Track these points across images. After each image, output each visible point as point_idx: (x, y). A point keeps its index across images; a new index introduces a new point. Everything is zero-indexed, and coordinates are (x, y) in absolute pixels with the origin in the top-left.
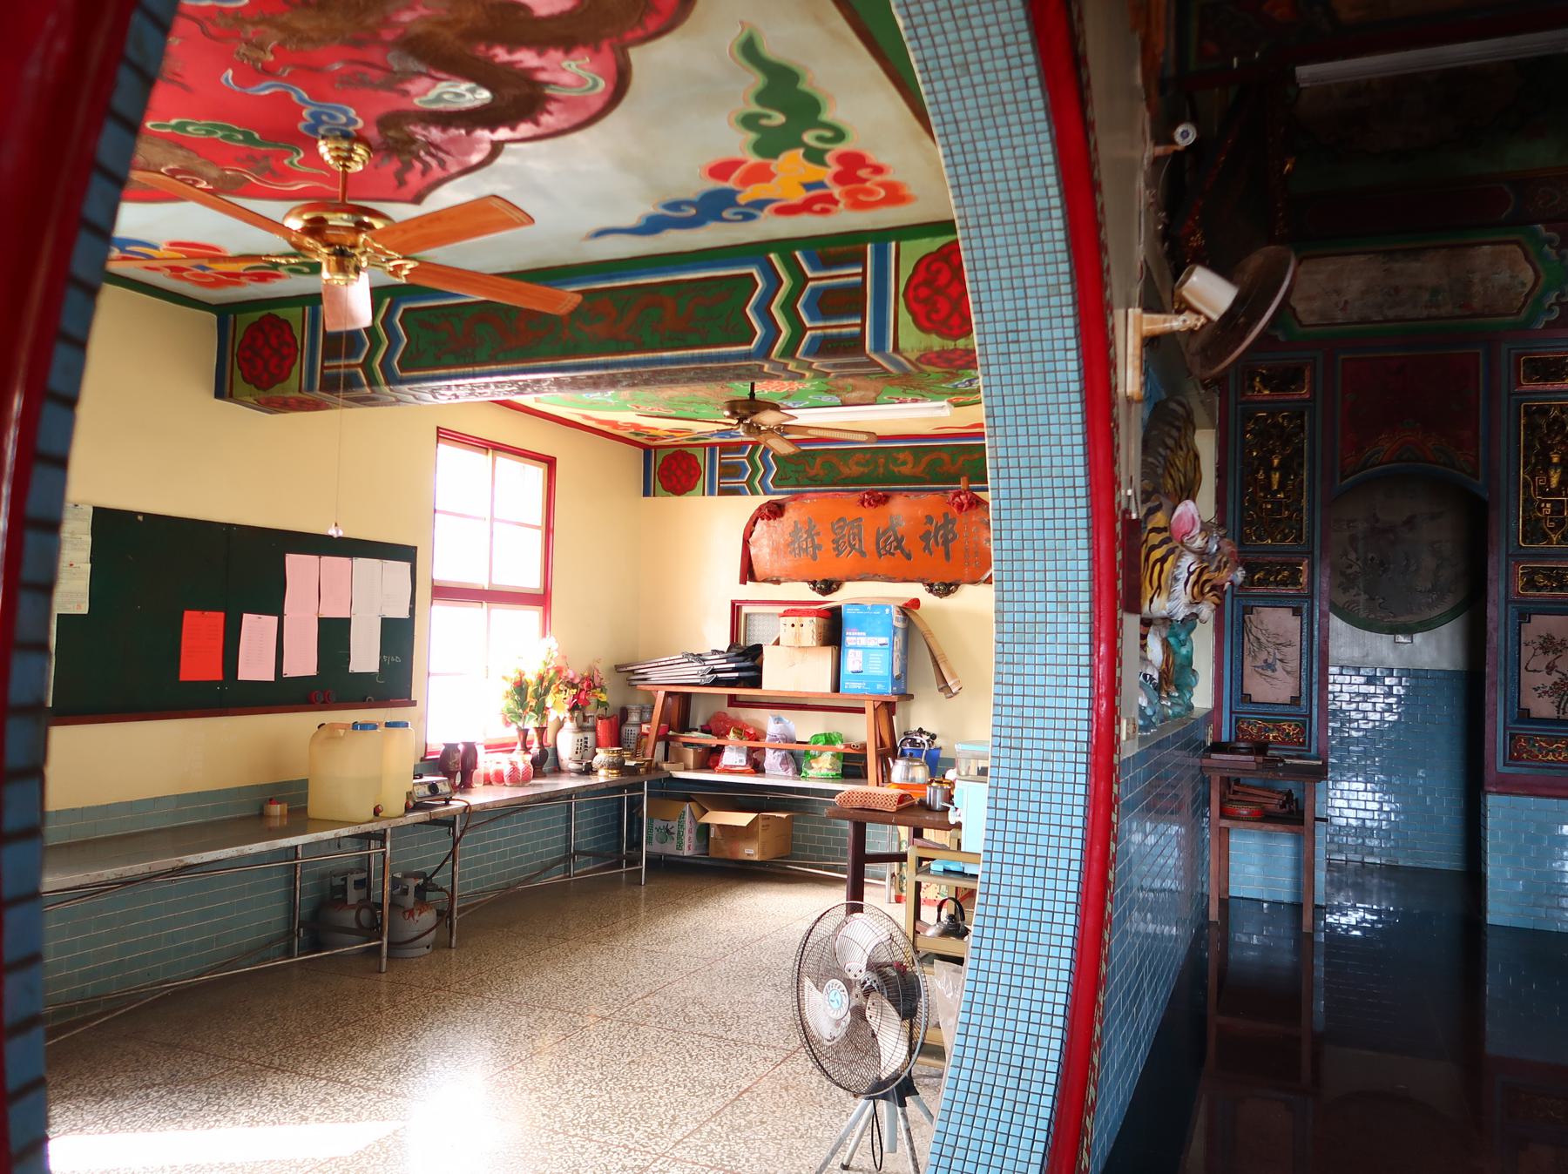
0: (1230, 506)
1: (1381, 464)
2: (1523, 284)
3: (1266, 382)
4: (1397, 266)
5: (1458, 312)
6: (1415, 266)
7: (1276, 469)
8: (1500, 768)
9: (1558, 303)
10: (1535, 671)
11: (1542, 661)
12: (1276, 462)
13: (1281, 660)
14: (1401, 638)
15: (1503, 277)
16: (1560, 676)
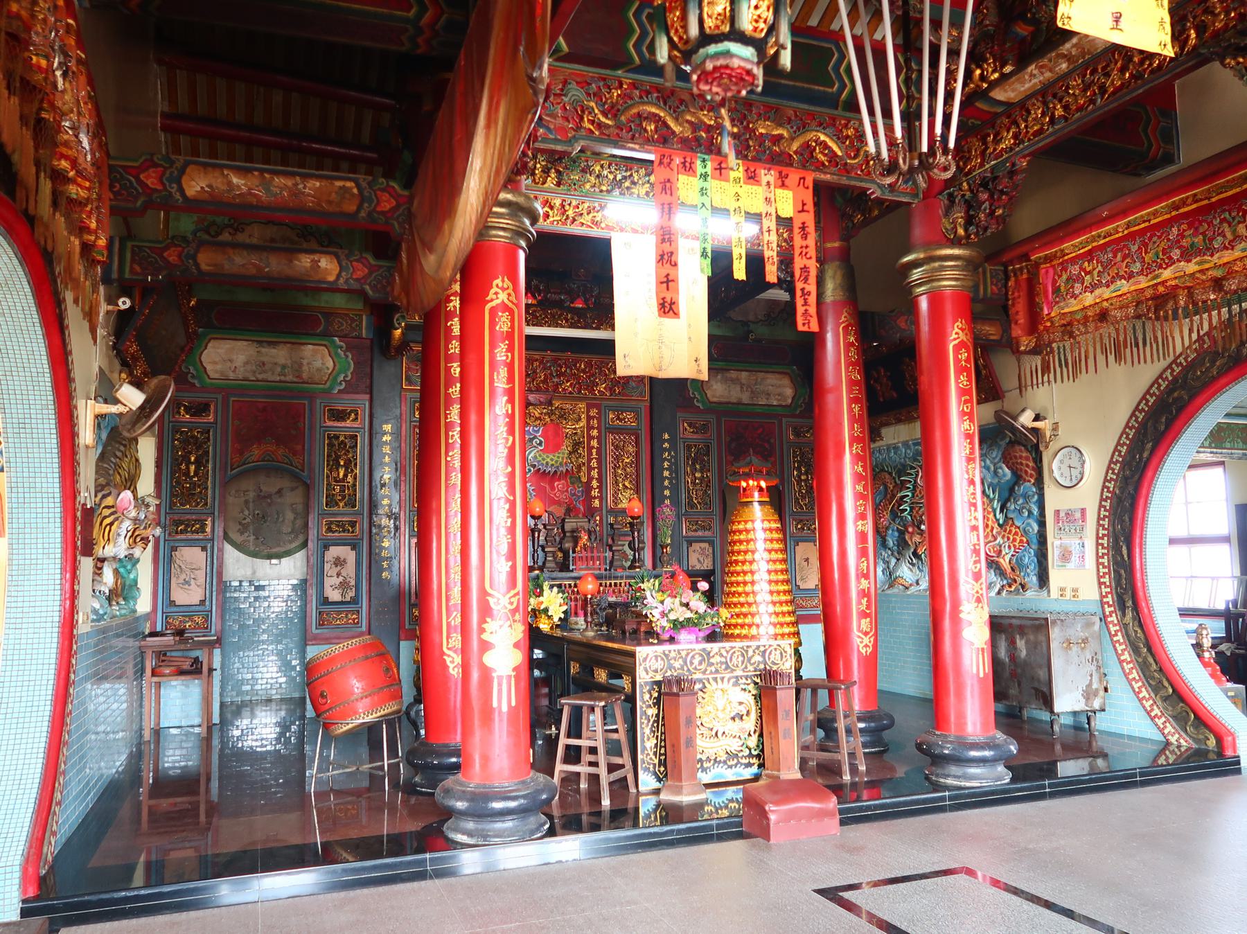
0: (164, 485)
2: (328, 369)
3: (187, 410)
4: (263, 350)
5: (295, 380)
6: (273, 351)
7: (193, 463)
8: (314, 631)
9: (344, 380)
11: (335, 570)
12: (193, 459)
14: (274, 561)
15: (318, 364)
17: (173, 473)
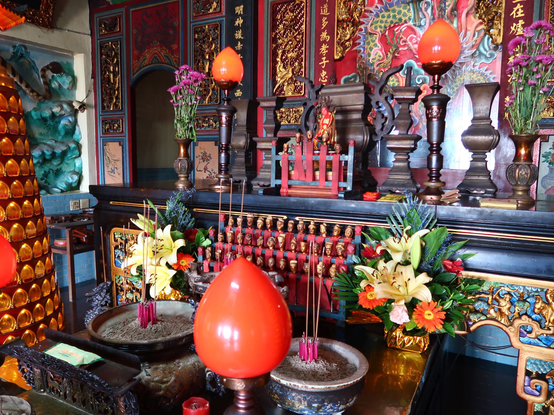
1: (146, 66)
10: (200, 171)
13: (116, 168)
16: (209, 173)
17: (102, 84)
